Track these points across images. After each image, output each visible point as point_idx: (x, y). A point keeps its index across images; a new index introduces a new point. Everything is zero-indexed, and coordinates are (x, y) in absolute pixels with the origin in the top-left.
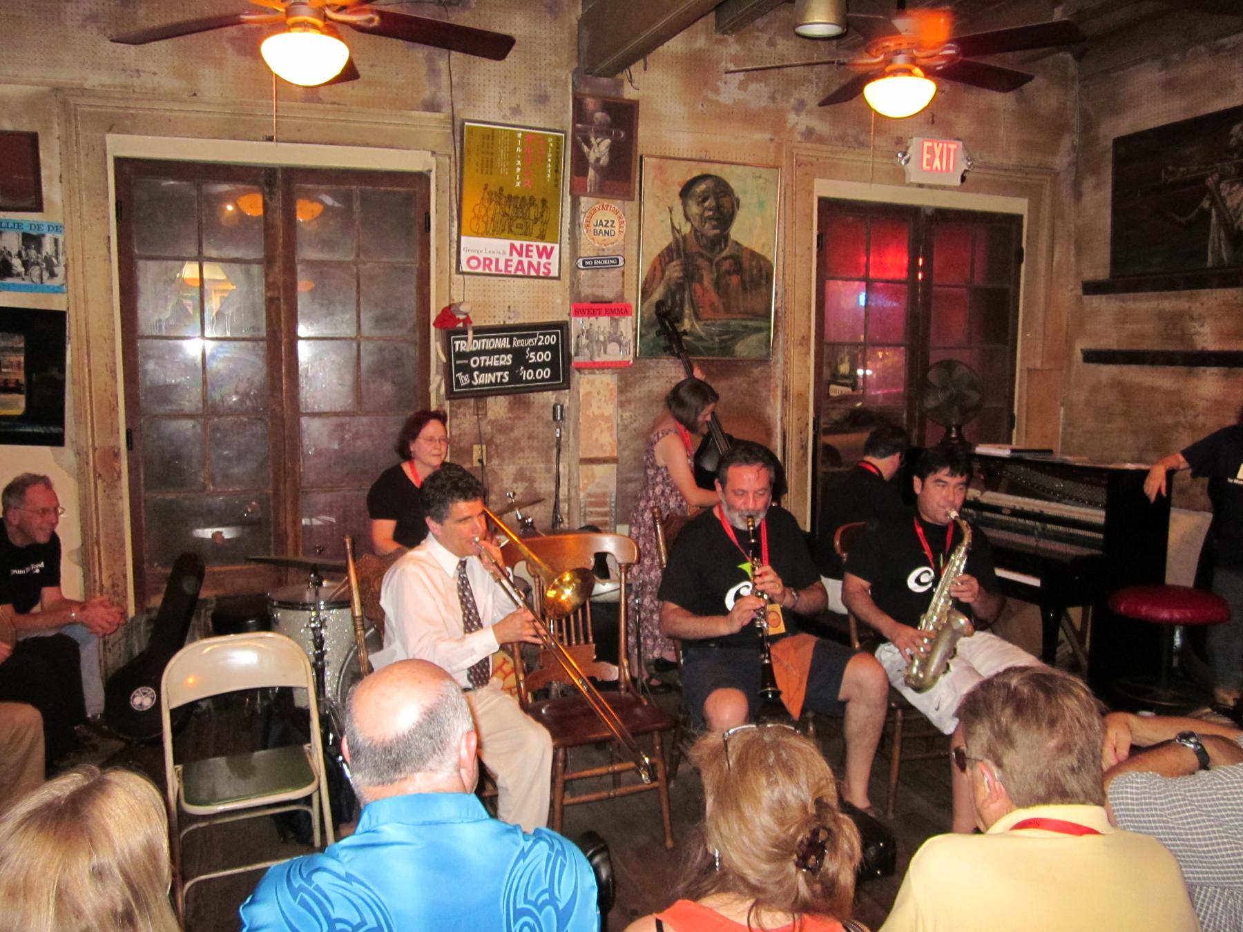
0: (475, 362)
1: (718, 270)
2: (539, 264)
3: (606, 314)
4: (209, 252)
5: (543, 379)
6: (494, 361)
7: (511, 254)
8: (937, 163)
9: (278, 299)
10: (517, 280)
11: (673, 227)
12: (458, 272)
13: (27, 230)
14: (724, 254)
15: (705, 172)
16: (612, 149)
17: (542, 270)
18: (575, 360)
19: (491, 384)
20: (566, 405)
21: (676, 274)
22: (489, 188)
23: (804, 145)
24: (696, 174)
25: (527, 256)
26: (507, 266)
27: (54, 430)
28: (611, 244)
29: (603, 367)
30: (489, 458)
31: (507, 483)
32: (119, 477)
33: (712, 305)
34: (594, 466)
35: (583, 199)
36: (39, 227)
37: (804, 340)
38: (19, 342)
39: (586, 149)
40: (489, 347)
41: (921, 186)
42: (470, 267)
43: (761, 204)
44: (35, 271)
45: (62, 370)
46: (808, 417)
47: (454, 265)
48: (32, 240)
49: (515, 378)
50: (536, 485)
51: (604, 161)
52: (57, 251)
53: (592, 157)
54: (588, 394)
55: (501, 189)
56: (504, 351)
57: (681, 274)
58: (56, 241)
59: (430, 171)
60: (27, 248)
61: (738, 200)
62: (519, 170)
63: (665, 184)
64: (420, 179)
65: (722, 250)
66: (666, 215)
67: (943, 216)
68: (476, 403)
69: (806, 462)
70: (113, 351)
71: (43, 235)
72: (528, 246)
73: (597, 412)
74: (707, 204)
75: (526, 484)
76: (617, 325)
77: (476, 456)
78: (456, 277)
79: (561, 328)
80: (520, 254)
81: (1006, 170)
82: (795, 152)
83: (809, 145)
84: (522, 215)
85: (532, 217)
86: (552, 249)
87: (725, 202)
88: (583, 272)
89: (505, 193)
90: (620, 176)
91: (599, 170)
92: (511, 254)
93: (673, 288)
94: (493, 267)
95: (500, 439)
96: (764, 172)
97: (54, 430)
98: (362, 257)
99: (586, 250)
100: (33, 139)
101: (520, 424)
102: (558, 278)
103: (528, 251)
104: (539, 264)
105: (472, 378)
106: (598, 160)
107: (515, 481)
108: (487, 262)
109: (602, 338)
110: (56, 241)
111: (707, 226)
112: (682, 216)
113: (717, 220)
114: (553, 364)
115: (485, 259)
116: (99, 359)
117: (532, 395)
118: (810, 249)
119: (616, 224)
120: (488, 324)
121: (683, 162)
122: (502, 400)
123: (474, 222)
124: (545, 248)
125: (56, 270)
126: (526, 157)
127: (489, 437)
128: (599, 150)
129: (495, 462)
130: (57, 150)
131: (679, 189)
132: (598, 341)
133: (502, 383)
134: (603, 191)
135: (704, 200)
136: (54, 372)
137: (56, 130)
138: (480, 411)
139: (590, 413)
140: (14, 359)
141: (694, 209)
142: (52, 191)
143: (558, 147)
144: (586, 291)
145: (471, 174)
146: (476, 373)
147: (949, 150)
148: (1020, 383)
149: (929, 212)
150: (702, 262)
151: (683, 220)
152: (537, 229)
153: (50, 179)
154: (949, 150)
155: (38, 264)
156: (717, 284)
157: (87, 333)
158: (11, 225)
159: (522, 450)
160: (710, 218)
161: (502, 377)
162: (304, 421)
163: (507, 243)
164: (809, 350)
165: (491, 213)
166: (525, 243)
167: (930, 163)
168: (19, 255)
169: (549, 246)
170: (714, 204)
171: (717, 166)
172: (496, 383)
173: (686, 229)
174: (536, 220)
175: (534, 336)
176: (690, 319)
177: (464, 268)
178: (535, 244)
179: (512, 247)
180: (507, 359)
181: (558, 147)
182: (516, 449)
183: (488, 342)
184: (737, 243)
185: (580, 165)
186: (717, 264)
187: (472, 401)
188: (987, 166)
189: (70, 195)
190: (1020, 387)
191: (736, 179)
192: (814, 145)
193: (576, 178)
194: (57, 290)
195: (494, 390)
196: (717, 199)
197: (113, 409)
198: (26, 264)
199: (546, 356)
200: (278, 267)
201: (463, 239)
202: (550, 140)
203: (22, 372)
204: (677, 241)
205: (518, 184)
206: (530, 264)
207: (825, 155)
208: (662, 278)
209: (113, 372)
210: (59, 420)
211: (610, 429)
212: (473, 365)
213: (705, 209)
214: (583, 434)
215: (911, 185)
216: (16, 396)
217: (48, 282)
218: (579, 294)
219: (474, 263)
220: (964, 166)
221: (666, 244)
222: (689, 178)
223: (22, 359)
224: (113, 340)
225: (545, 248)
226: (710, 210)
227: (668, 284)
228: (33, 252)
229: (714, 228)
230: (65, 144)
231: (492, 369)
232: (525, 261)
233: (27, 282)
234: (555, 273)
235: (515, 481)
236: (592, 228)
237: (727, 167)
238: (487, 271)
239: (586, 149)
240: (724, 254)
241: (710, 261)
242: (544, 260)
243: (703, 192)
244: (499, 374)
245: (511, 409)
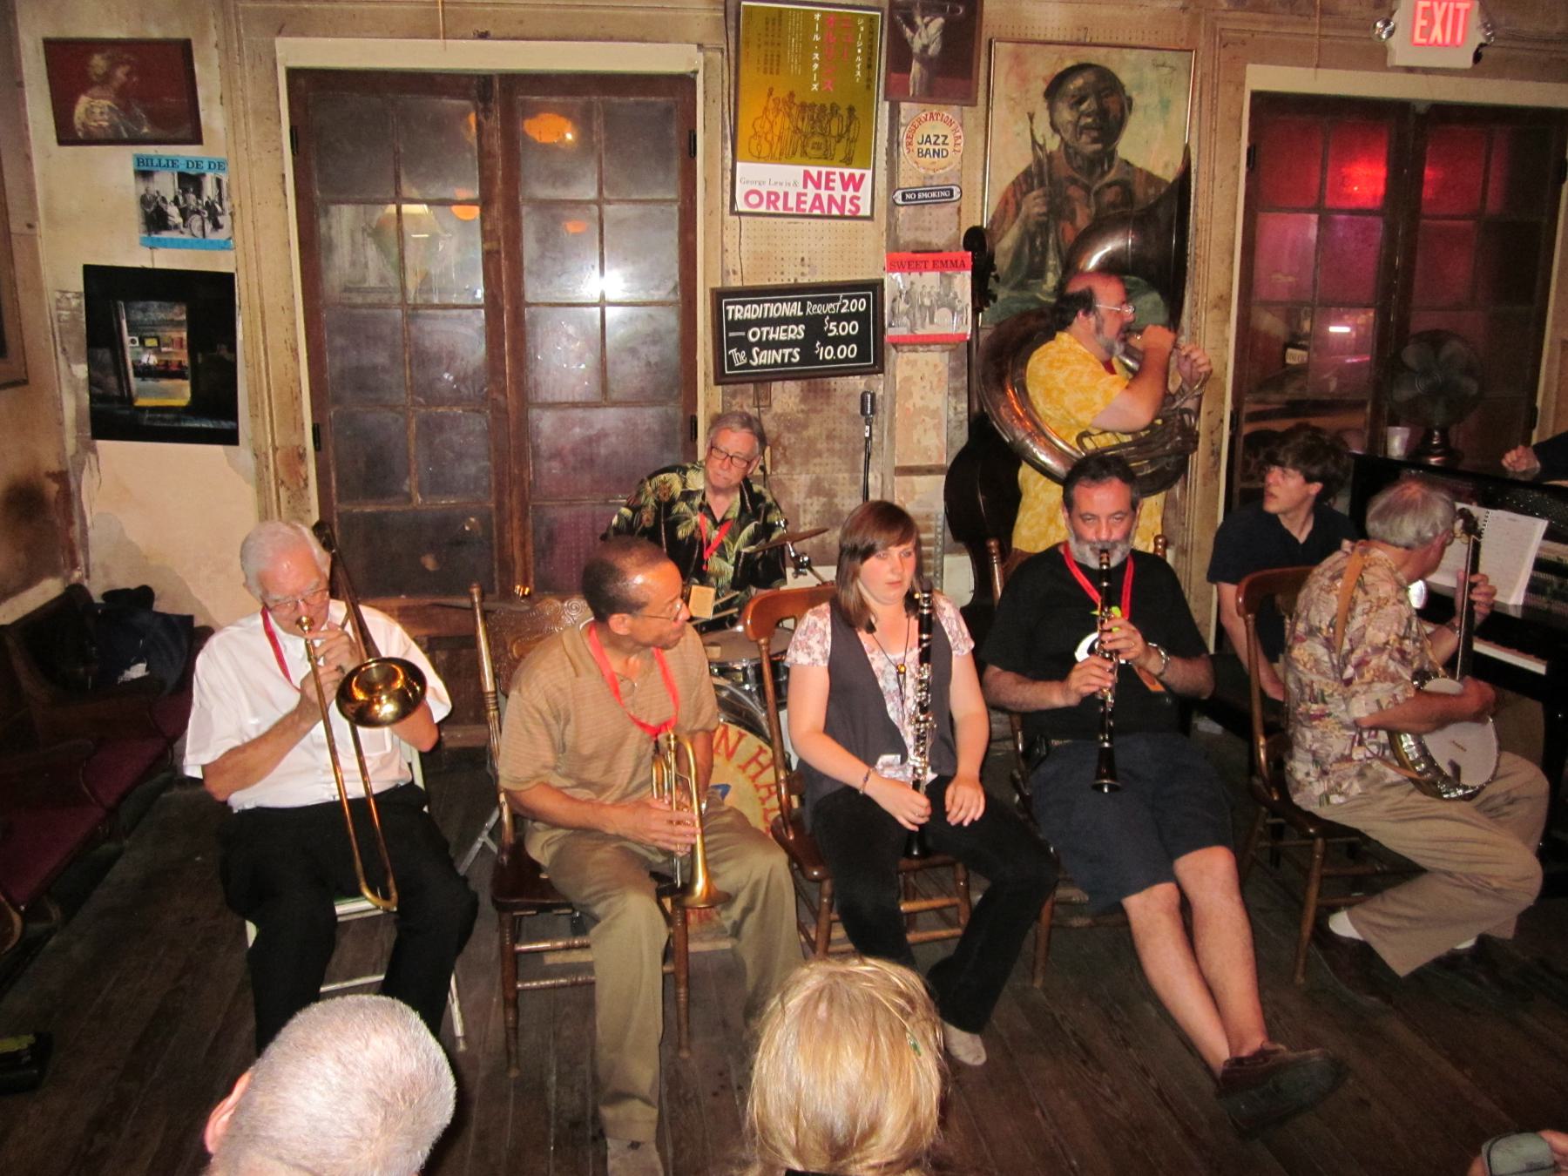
0: (754, 335)
1: (1098, 203)
2: (843, 198)
3: (934, 268)
4: (408, 190)
5: (847, 360)
6: (780, 334)
7: (805, 186)
8: (1437, 32)
9: (498, 252)
10: (812, 221)
11: (1034, 142)
12: (733, 212)
13: (183, 168)
14: (1109, 178)
15: (1083, 60)
16: (946, 31)
17: (848, 206)
18: (890, 332)
19: (776, 364)
20: (879, 394)
21: (1036, 210)
22: (775, 95)
23: (1231, 15)
24: (1069, 63)
25: (828, 188)
26: (799, 202)
27: (226, 425)
28: (942, 169)
29: (927, 342)
30: (774, 464)
31: (798, 497)
32: (306, 485)
34: (915, 478)
35: (904, 106)
36: (198, 164)
37: (1224, 300)
38: (180, 313)
39: (908, 33)
40: (773, 314)
41: (1410, 70)
42: (750, 205)
43: (1165, 105)
44: (196, 221)
45: (232, 348)
46: (1223, 410)
47: (728, 202)
48: (190, 182)
50: (836, 501)
51: (934, 49)
52: (220, 194)
53: (917, 45)
54: (907, 379)
55: (792, 95)
56: (795, 320)
57: (1044, 209)
58: (219, 182)
59: (696, 72)
60: (185, 191)
61: (1130, 100)
62: (816, 66)
63: (1024, 79)
64: (682, 84)
65: (1104, 174)
66: (1024, 125)
67: (1443, 113)
68: (756, 390)
69: (1217, 473)
70: (294, 324)
71: (204, 175)
72: (828, 174)
73: (920, 403)
74: (1084, 107)
75: (823, 500)
76: (950, 283)
78: (731, 220)
79: (876, 287)
80: (818, 186)
81: (1546, 42)
82: (1219, 25)
83: (1238, 14)
84: (827, 131)
85: (834, 132)
86: (862, 177)
87: (1112, 104)
88: (902, 210)
89: (797, 100)
90: (956, 72)
91: (926, 62)
92: (805, 186)
93: (1033, 229)
94: (780, 204)
95: (788, 439)
96: (1169, 57)
97: (226, 425)
98: (606, 193)
99: (907, 179)
100: (185, 47)
101: (815, 418)
102: (870, 218)
103: (828, 180)
104: (843, 198)
105: (749, 356)
106: (925, 48)
107: (809, 495)
108: (772, 198)
109: (927, 302)
110: (219, 182)
111: (1084, 138)
112: (1048, 124)
113: (1099, 129)
114: (861, 339)
115: (769, 194)
116: (277, 335)
117: (833, 380)
118: (1236, 168)
119: (950, 140)
120: (773, 282)
121: (1051, 47)
122: (790, 385)
123: (754, 142)
124: (852, 176)
125: (220, 219)
126: (825, 47)
127: (774, 436)
128: (927, 34)
129: (782, 469)
130: (216, 62)
131: (1043, 86)
132: (922, 306)
133: (790, 364)
134: (932, 93)
135: (1080, 101)
136: (223, 351)
137: (213, 36)
138: (763, 399)
139: (909, 405)
140: (175, 335)
141: (1066, 115)
142: (212, 116)
143: (871, 32)
144: (906, 236)
145: (749, 73)
146: (755, 349)
147: (1457, 11)
148: (1550, 361)
149: (1421, 109)
150: (1074, 192)
151: (1049, 131)
152: (840, 153)
153: (209, 100)
154: (1457, 11)
155: (198, 212)
157: (261, 298)
158: (164, 162)
159: (820, 455)
160: (1087, 127)
161: (791, 355)
162: (534, 413)
163: (801, 169)
164: (1229, 313)
165: (777, 130)
166: (824, 170)
167: (1426, 32)
168: (176, 201)
169: (857, 173)
170: (1094, 106)
171: (1103, 51)
172: (783, 364)
173: (1053, 144)
174: (840, 137)
175: (835, 299)
177: (741, 206)
178: (838, 170)
179: (807, 175)
180: (798, 332)
181: (871, 32)
182: (810, 452)
183: (773, 308)
184: (1128, 163)
185: (900, 56)
186: (1097, 193)
187: (751, 387)
188: (1514, 37)
189: (233, 124)
190: (1548, 369)
191: (1128, 69)
192: (1246, 15)
193: (895, 76)
194: (224, 246)
195: (781, 373)
196: (1099, 99)
197: (297, 398)
198: (184, 213)
199: (851, 328)
200: (497, 210)
201: (739, 165)
202: (861, 22)
203: (185, 351)
204: (1039, 162)
205: (815, 87)
206: (831, 199)
207: (1264, 28)
208: (1017, 215)
209: (295, 351)
210: (233, 416)
211: (937, 427)
212: (752, 339)
213: (1082, 114)
214: (899, 434)
215: (1397, 69)
216: (179, 382)
217: (212, 236)
218: (896, 240)
219: (754, 199)
220: (1480, 39)
221: (1022, 167)
222: (1060, 70)
223: (185, 335)
224: (293, 310)
225: (852, 176)
226: (1088, 115)
227: (1025, 222)
228: (192, 198)
229: (1095, 141)
230: (226, 53)
232: (824, 194)
233: (187, 236)
234: (865, 211)
235: (809, 495)
236: (915, 146)
237: (1115, 54)
238: (772, 210)
239: (908, 33)
240: (1109, 178)
241: (1087, 189)
242: (850, 193)
243: (1080, 89)
244: (787, 351)
245: (804, 400)
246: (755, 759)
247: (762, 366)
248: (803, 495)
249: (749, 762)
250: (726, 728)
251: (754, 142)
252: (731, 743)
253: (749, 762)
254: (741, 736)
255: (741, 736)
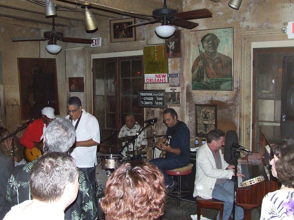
0: (145, 98)
14: (216, 57)
33: (212, 74)
49: (154, 104)
61: (219, 40)
65: (215, 56)
87: (215, 41)
156: (214, 67)
161: (151, 103)
176: (206, 78)
180: (152, 99)
231: (148, 101)
240: (216, 57)
241: (211, 60)
247: (146, 105)
251: (147, 70)
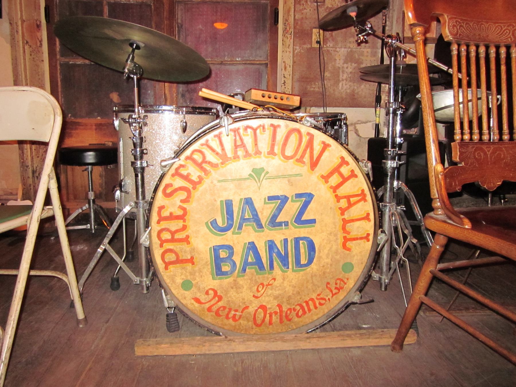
30: (325, 40)
31: (339, 63)
75: (354, 65)
77: (315, 38)
107: (346, 62)
129: (330, 44)
235: (346, 62)
246: (336, 170)
248: (342, 62)
249: (331, 174)
250: (312, 137)
252: (316, 153)
253: (331, 174)
254: (326, 146)
255: (326, 146)
